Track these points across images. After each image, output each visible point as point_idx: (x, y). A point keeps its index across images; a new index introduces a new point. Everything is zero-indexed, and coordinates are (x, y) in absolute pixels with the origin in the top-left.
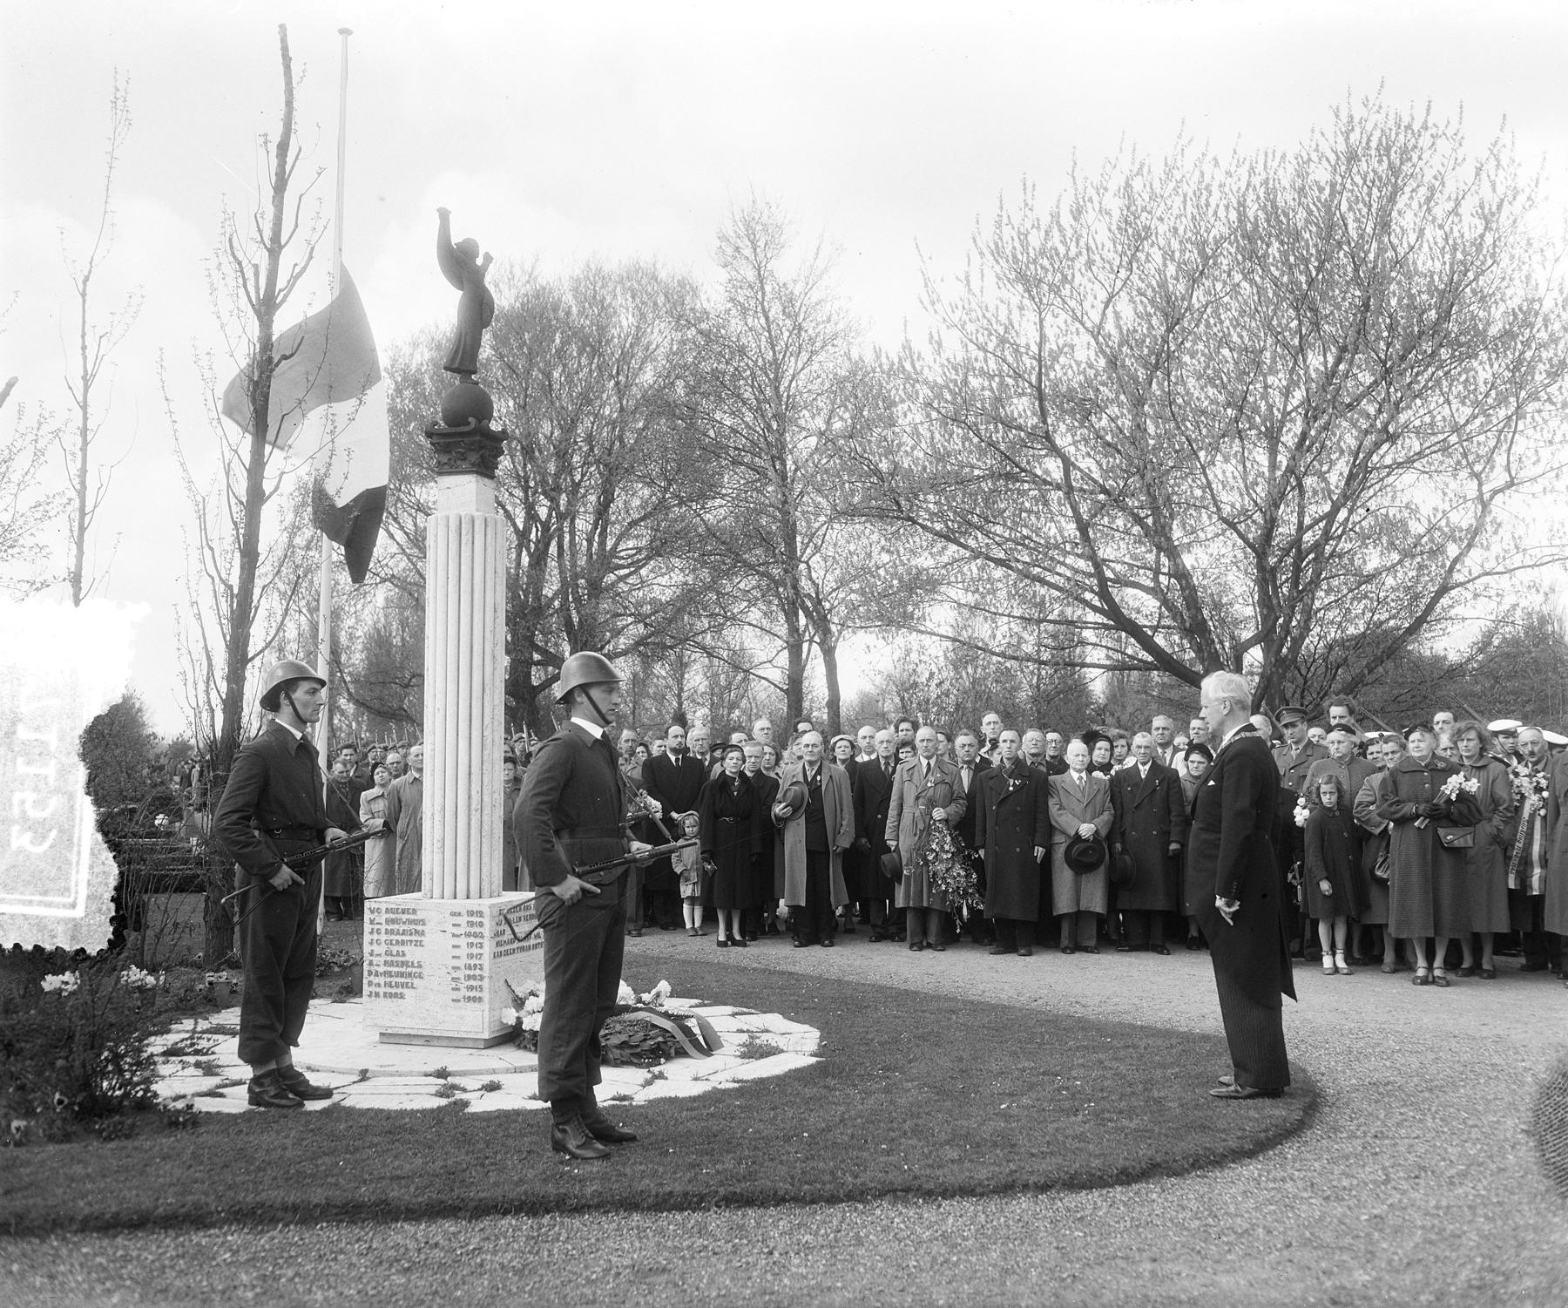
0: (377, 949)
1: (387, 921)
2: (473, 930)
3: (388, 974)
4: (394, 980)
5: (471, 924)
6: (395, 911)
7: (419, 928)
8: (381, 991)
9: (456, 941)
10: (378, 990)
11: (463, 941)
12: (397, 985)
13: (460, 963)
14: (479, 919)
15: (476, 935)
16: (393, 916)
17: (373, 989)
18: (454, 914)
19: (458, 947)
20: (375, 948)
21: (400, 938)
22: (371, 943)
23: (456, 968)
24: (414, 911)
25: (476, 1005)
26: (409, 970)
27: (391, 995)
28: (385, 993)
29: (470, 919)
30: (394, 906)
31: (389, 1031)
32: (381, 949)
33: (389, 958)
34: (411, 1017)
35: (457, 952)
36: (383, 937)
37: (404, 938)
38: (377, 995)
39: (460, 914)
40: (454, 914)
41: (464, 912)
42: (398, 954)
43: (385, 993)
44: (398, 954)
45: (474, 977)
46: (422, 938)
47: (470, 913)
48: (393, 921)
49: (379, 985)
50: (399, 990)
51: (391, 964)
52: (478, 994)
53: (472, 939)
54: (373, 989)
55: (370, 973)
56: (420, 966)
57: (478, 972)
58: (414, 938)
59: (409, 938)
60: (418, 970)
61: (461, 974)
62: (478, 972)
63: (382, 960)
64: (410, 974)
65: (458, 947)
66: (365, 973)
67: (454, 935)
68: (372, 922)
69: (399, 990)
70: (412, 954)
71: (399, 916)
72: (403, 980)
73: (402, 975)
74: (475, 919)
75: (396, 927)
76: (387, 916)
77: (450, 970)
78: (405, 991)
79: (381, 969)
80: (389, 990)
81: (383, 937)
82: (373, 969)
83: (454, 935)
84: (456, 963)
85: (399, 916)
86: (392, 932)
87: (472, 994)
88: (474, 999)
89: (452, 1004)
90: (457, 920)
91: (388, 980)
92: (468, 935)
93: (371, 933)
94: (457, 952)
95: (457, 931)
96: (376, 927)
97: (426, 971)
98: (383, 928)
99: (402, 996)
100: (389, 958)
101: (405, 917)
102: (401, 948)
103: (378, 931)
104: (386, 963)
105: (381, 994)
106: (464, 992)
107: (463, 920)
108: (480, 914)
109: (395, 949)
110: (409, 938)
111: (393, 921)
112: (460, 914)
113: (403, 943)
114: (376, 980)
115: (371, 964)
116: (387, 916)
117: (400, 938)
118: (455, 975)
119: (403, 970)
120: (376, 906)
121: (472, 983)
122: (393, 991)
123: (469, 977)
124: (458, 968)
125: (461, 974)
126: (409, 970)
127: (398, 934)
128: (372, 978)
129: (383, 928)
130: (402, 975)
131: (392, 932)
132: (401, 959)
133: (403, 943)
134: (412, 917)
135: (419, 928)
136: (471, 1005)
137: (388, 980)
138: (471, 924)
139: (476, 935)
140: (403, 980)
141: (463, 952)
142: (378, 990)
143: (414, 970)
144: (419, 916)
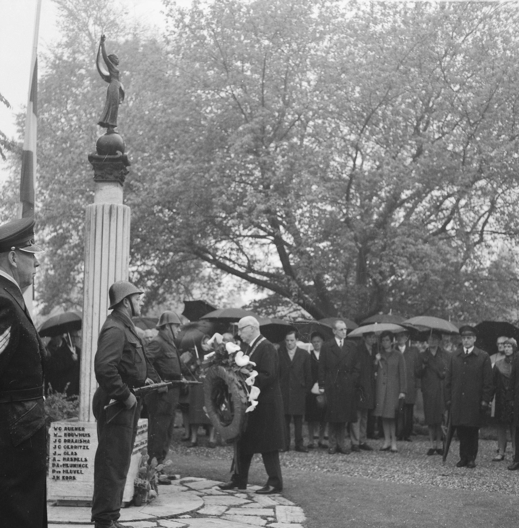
0: (58, 451)
1: (65, 435)
3: (67, 465)
4: (69, 469)
6: (69, 429)
7: (86, 438)
8: (61, 475)
10: (58, 475)
12: (71, 472)
16: (70, 432)
17: (56, 474)
20: (58, 451)
21: (73, 444)
22: (55, 447)
31: (66, 499)
33: (67, 457)
34: (80, 490)
37: (77, 444)
43: (63, 477)
44: (72, 453)
49: (60, 472)
50: (73, 475)
51: (68, 460)
54: (56, 474)
55: (54, 465)
56: (86, 460)
58: (82, 444)
60: (85, 463)
64: (80, 466)
66: (51, 465)
68: (55, 435)
69: (73, 475)
71: (73, 432)
72: (75, 469)
73: (75, 466)
75: (71, 438)
78: (76, 475)
79: (61, 463)
81: (63, 444)
82: (56, 463)
85: (73, 432)
86: (69, 441)
91: (65, 469)
93: (55, 441)
96: (58, 438)
98: (63, 439)
99: (74, 478)
100: (67, 457)
101: (77, 432)
102: (74, 451)
103: (60, 441)
104: (64, 459)
105: (61, 478)
109: (70, 451)
111: (69, 435)
113: (76, 447)
115: (54, 459)
116: (66, 432)
117: (73, 444)
119: (76, 463)
120: (59, 426)
122: (69, 475)
126: (79, 463)
127: (72, 441)
129: (63, 439)
130: (75, 466)
131: (69, 441)
132: (73, 457)
133: (76, 447)
134: (82, 432)
135: (86, 438)
137: (65, 469)
140: (75, 469)
142: (58, 475)
143: (82, 463)
144: (86, 431)
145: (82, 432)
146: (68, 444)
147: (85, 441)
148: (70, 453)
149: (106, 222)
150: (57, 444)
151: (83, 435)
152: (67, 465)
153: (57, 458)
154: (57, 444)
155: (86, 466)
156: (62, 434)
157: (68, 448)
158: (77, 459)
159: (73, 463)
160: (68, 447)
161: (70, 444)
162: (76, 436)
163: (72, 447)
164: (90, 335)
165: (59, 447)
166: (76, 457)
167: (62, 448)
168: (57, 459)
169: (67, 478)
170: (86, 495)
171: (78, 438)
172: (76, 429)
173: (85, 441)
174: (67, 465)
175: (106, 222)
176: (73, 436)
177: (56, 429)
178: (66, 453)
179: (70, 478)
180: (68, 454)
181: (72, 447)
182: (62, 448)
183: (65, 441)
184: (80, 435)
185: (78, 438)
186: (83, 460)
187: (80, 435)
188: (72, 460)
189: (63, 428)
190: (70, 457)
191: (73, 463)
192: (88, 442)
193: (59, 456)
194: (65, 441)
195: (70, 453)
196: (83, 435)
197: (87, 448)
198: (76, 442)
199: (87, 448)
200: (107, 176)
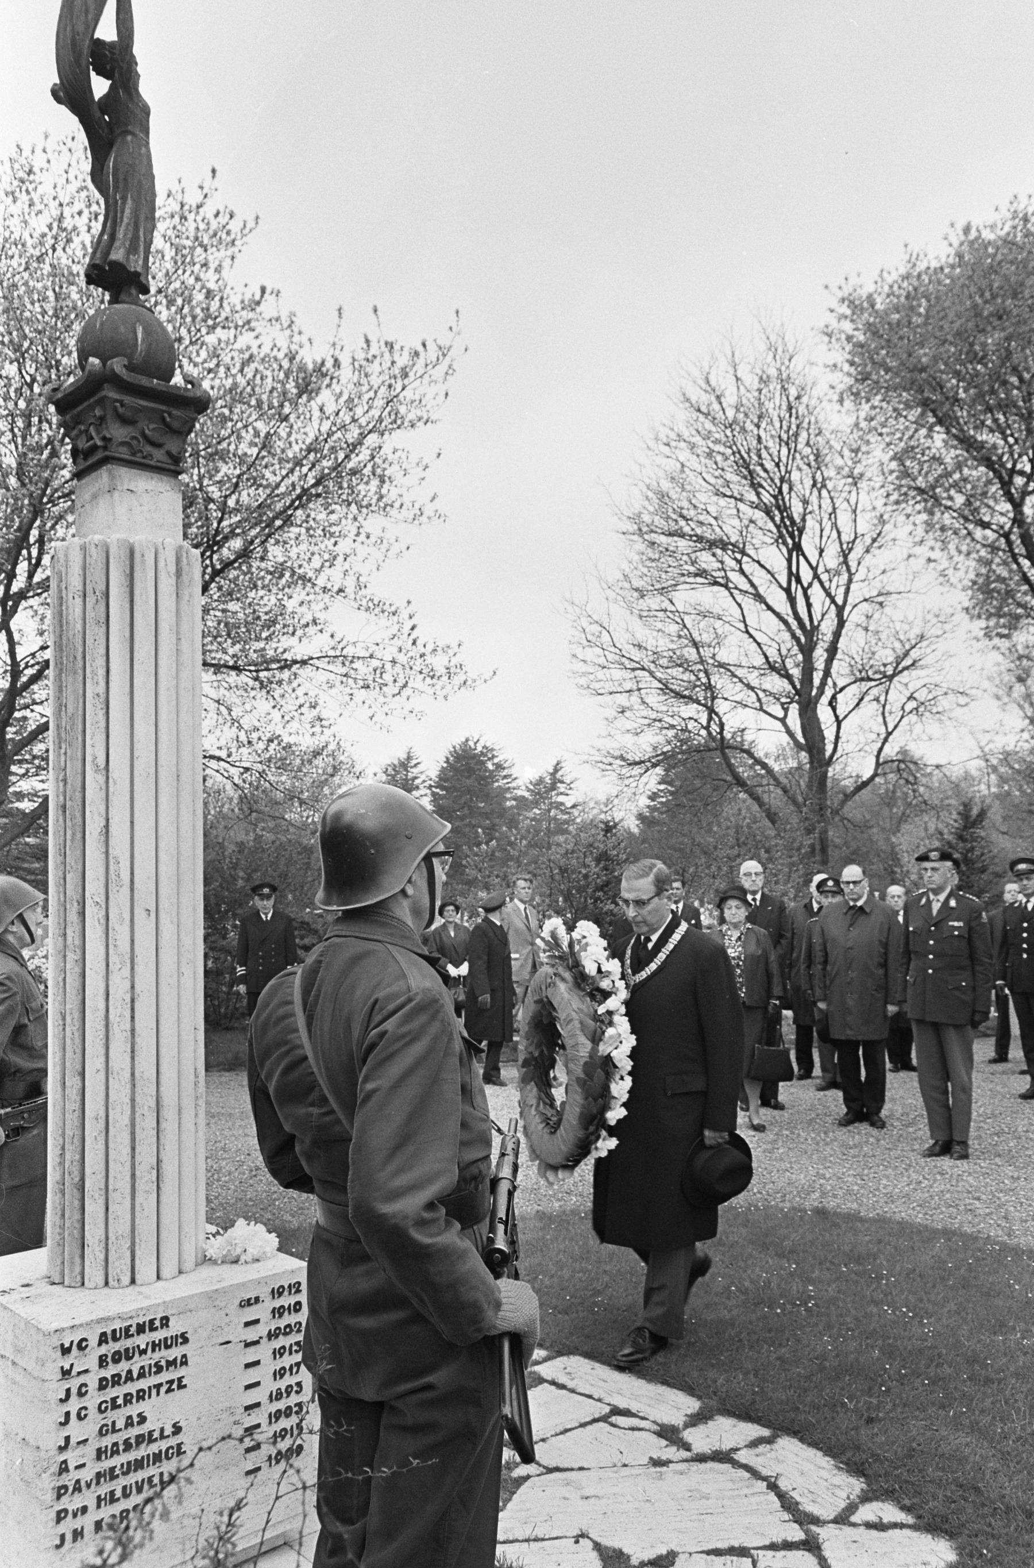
1: (102, 1362)
2: (282, 1323)
3: (111, 1474)
4: (117, 1485)
7: (175, 1353)
9: (251, 1355)
10: (77, 1524)
13: (259, 1395)
15: (288, 1330)
17: (68, 1526)
18: (248, 1303)
20: (76, 1430)
21: (132, 1388)
24: (165, 1321)
26: (154, 1448)
29: (277, 1303)
30: (117, 1325)
35: (252, 1375)
36: (93, 1399)
37: (144, 1384)
38: (78, 1534)
39: (257, 1300)
40: (248, 1303)
41: (264, 1293)
42: (129, 1423)
44: (129, 1423)
46: (182, 1372)
47: (278, 1292)
48: (117, 1358)
54: (68, 1526)
55: (60, 1492)
58: (164, 1377)
60: (173, 1441)
61: (259, 1417)
63: (90, 1450)
71: (129, 1343)
73: (139, 1464)
75: (123, 1367)
76: (104, 1349)
79: (87, 1475)
83: (248, 1345)
85: (129, 1343)
86: (116, 1380)
90: (250, 1314)
91: (104, 1490)
92: (272, 1335)
94: (252, 1375)
95: (251, 1335)
96: (74, 1384)
100: (108, 1441)
101: (142, 1341)
102: (134, 1410)
104: (100, 1454)
106: (267, 1450)
107: (261, 1311)
108: (296, 1288)
109: (119, 1417)
111: (117, 1358)
113: (141, 1395)
116: (104, 1349)
117: (132, 1388)
123: (278, 1415)
124: (258, 1405)
126: (154, 1448)
128: (65, 1503)
129: (92, 1381)
130: (139, 1464)
131: (116, 1380)
134: (159, 1335)
135: (175, 1353)
137: (104, 1490)
142: (77, 1524)
143: (163, 1445)
144: (175, 1328)
145: (159, 1335)
146: (111, 1393)
147: (172, 1363)
148: (120, 1424)
149: (167, 602)
153: (72, 1457)
154: (74, 1405)
156: (91, 1361)
157: (115, 1406)
161: (119, 1392)
171: (146, 1361)
172: (141, 1329)
173: (172, 1363)
174: (111, 1474)
175: (167, 602)
177: (65, 1351)
180: (114, 1431)
181: (128, 1399)
182: (93, 1411)
183: (103, 1384)
184: (155, 1346)
185: (146, 1361)
187: (155, 1346)
189: (93, 1341)
190: (120, 1438)
195: (120, 1424)
197: (181, 1387)
198: (142, 1375)
199: (181, 1387)
200: (148, 449)
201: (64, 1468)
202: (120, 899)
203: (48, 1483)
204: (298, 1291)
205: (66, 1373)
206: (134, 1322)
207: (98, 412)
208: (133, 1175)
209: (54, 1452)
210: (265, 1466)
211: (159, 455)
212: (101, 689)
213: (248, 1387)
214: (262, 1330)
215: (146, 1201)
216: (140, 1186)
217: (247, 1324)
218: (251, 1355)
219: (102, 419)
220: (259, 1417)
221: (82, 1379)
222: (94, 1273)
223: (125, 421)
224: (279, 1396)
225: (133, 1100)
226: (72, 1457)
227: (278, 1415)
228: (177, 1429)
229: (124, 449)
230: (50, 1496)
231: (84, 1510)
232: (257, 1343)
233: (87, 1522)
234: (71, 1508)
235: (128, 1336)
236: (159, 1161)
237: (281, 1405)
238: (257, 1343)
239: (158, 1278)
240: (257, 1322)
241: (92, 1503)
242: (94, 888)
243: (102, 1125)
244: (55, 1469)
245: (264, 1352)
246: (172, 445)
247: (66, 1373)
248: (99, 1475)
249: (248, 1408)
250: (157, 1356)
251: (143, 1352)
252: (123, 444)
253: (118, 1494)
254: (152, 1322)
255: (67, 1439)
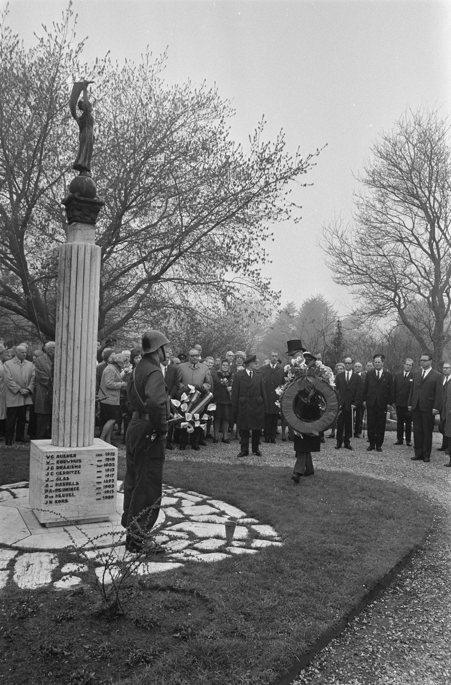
0: (51, 478)
1: (58, 462)
2: (109, 463)
3: (59, 490)
4: (61, 493)
5: (108, 459)
7: (78, 464)
8: (54, 500)
9: (99, 469)
10: (51, 499)
11: (103, 469)
12: (63, 496)
14: (112, 457)
15: (110, 465)
17: (48, 499)
18: (98, 455)
19: (101, 472)
20: (51, 478)
21: (66, 470)
23: (98, 483)
24: (75, 456)
25: (110, 500)
27: (60, 501)
28: (56, 502)
29: (107, 457)
30: (62, 454)
32: (54, 477)
33: (59, 482)
35: (99, 475)
36: (55, 471)
38: (51, 502)
39: (101, 455)
40: (98, 455)
41: (104, 453)
43: (56, 502)
44: (64, 479)
45: (109, 486)
47: (108, 454)
48: (61, 462)
50: (64, 498)
51: (60, 485)
52: (111, 495)
53: (108, 467)
54: (48, 499)
55: (46, 491)
56: (77, 484)
57: (111, 483)
58: (74, 469)
59: (72, 470)
62: (111, 483)
63: (54, 483)
64: (72, 489)
65: (101, 472)
67: (98, 466)
70: (73, 478)
71: (65, 459)
72: (67, 492)
73: (67, 490)
74: (110, 457)
75: (63, 465)
76: (58, 459)
77: (95, 484)
78: (68, 498)
79: (53, 489)
80: (58, 499)
81: (55, 471)
82: (49, 488)
83: (98, 466)
84: (99, 480)
85: (65, 459)
86: (61, 468)
87: (108, 495)
88: (109, 497)
89: (95, 501)
90: (99, 458)
91: (58, 493)
92: (106, 465)
94: (99, 475)
95: (99, 464)
97: (80, 487)
99: (66, 501)
100: (59, 482)
101: (69, 459)
102: (66, 476)
103: (52, 468)
104: (57, 485)
105: (54, 501)
106: (103, 494)
107: (103, 458)
108: (113, 454)
109: (62, 477)
110: (72, 470)
111: (61, 462)
112: (101, 455)
113: (68, 473)
114: (50, 495)
115: (47, 486)
116: (58, 459)
117: (66, 470)
118: (98, 486)
121: (108, 489)
122: (61, 499)
123: (106, 486)
124: (100, 482)
125: (101, 486)
126: (71, 487)
127: (65, 467)
128: (47, 494)
130: (67, 490)
131: (61, 468)
132: (66, 481)
133: (68, 473)
134: (73, 459)
135: (78, 464)
136: (108, 500)
137: (58, 493)
138: (108, 459)
139: (110, 465)
141: (104, 474)
142: (51, 499)
143: (74, 487)
144: (78, 457)
145: (73, 459)
147: (76, 466)
148: (62, 478)
150: (50, 471)
151: (75, 461)
152: (60, 489)
153: (50, 484)
154: (50, 471)
155: (78, 489)
156: (55, 461)
157: (60, 474)
158: (70, 484)
159: (65, 487)
160: (60, 473)
162: (69, 462)
163: (64, 473)
164: (71, 367)
165: (52, 474)
166: (68, 481)
167: (55, 474)
168: (49, 485)
169: (60, 501)
170: (77, 515)
171: (70, 464)
172: (68, 456)
173: (76, 466)
174: (59, 490)
176: (65, 463)
177: (48, 457)
178: (57, 479)
179: (63, 501)
180: (60, 480)
181: (64, 473)
182: (55, 474)
183: (58, 468)
184: (72, 461)
185: (70, 464)
186: (75, 483)
187: (72, 461)
188: (64, 484)
189: (55, 456)
190: (62, 482)
191: (65, 487)
192: (80, 467)
193: (51, 483)
194: (58, 468)
195: (62, 478)
196: (75, 461)
197: (79, 473)
198: (68, 468)
199: (79, 473)
200: (86, 217)
201: (47, 486)
202: (71, 343)
203: (43, 488)
204: (114, 455)
205: (48, 463)
206: (66, 454)
207: (71, 208)
208: (71, 419)
209: (44, 481)
210: (102, 499)
211: (88, 219)
212: (68, 286)
213: (98, 477)
214: (102, 463)
215: (75, 426)
216: (73, 421)
217: (98, 461)
218: (99, 469)
219: (73, 210)
220: (101, 486)
221: (52, 465)
222: (61, 444)
223: (79, 210)
224: (107, 481)
225: (72, 398)
226: (50, 484)
227: (106, 486)
228: (77, 484)
229: (78, 218)
230: (43, 491)
231: (52, 497)
232: (100, 466)
233: (54, 500)
234: (49, 495)
235: (64, 457)
236: (78, 416)
237: (108, 484)
238: (100, 466)
239: (77, 446)
240: (101, 461)
241: (54, 495)
242: (64, 340)
243: (63, 404)
244: (45, 485)
245: (103, 469)
246: (93, 216)
247: (48, 463)
248: (56, 490)
249: (97, 483)
250: (72, 464)
251: (69, 462)
252: (79, 216)
253: (61, 495)
254: (71, 455)
255: (48, 479)
